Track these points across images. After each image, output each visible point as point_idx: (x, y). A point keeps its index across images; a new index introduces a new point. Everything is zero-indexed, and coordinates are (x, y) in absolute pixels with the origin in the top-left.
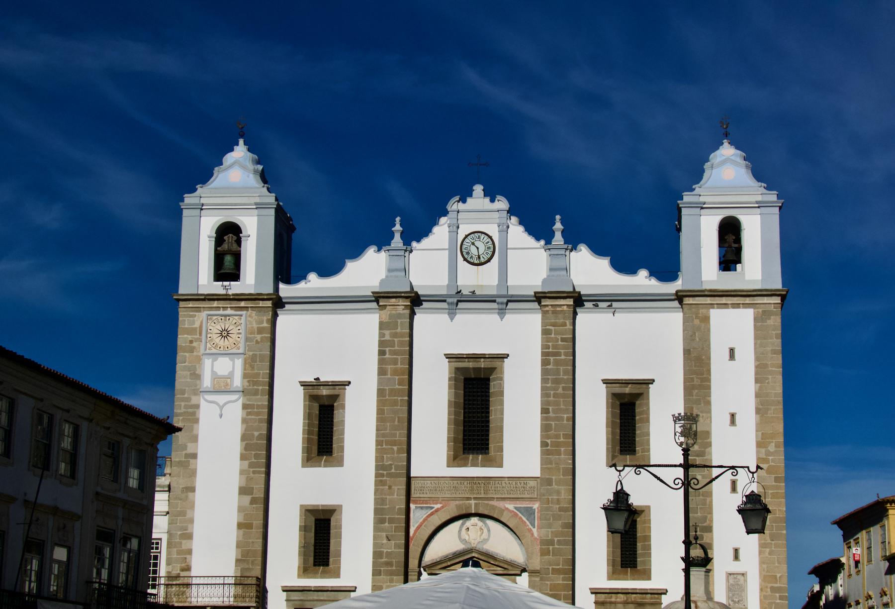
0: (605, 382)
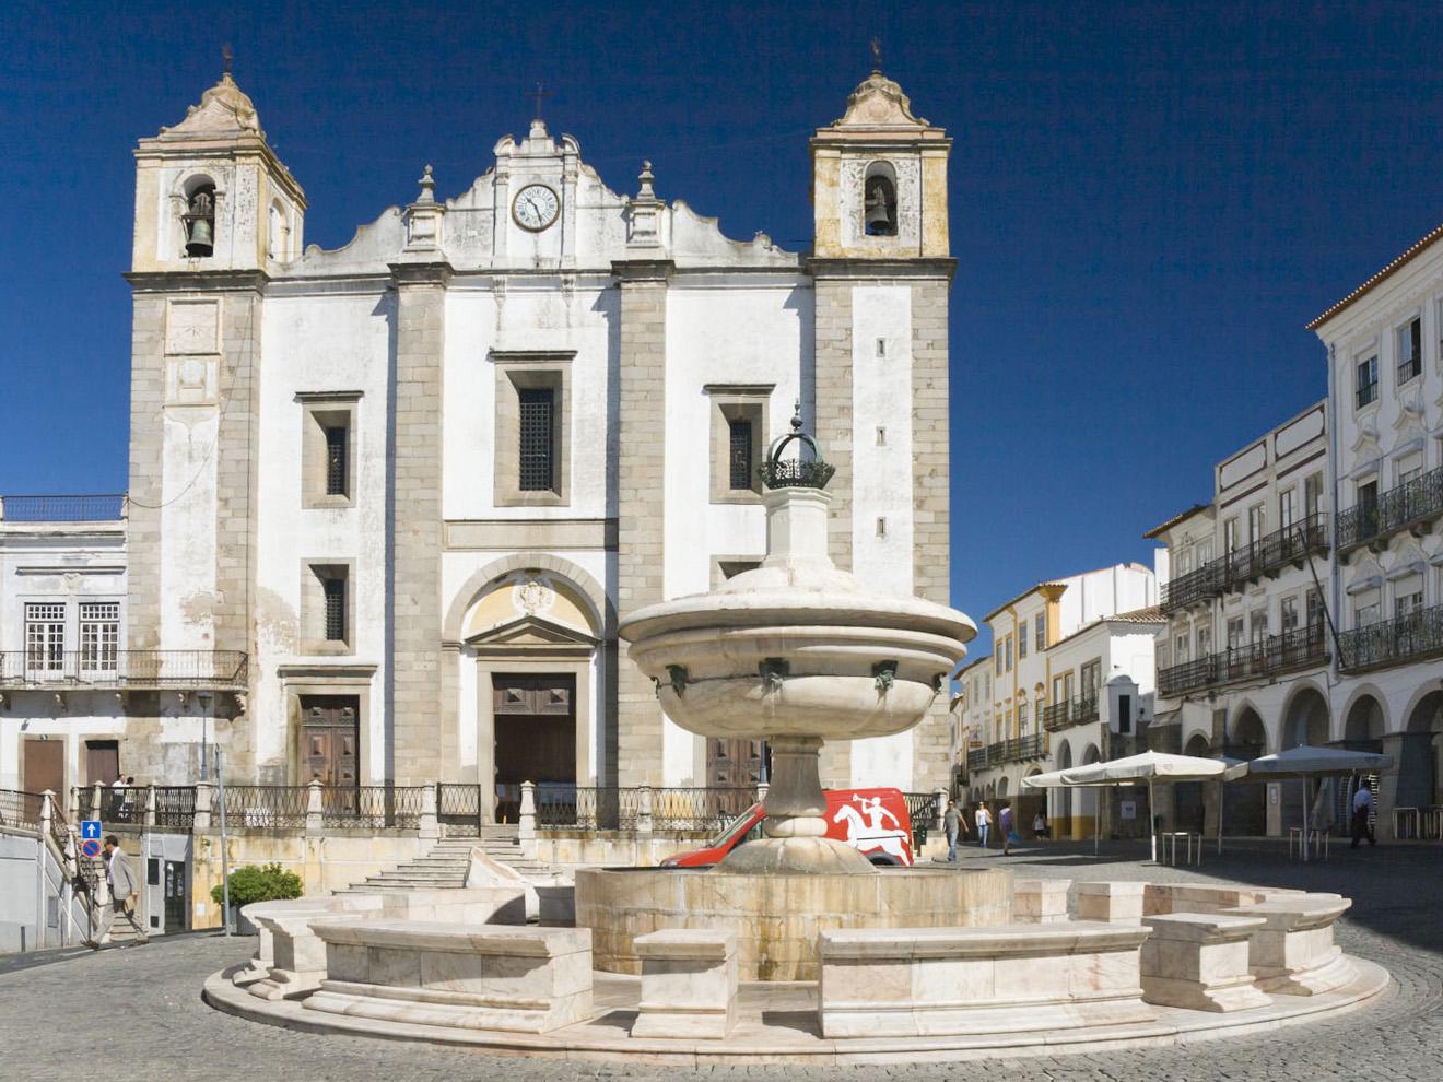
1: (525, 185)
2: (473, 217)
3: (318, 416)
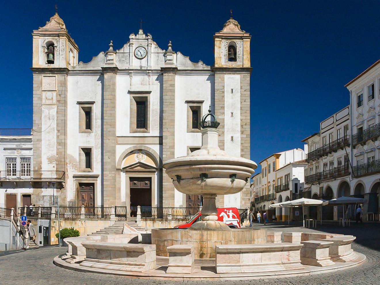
1: (138, 46)
2: (124, 55)
3: (83, 108)
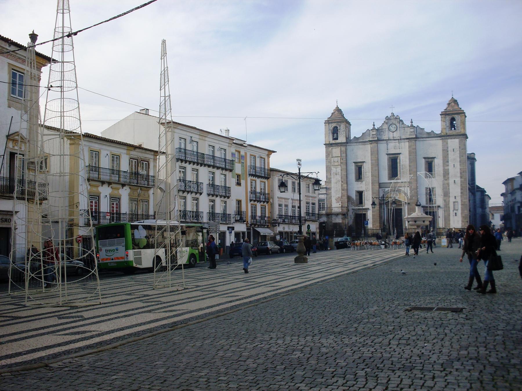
0: (425, 158)
3: (357, 166)
